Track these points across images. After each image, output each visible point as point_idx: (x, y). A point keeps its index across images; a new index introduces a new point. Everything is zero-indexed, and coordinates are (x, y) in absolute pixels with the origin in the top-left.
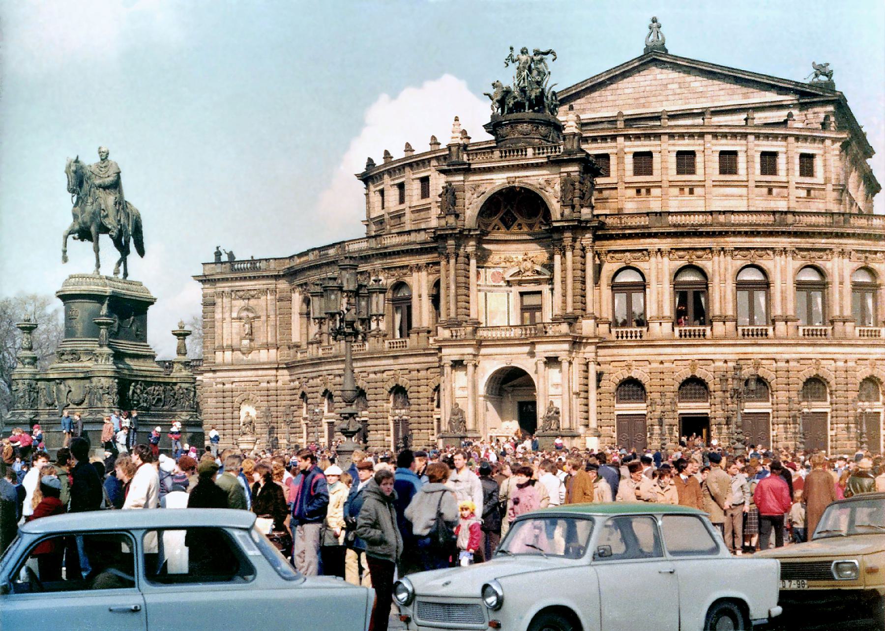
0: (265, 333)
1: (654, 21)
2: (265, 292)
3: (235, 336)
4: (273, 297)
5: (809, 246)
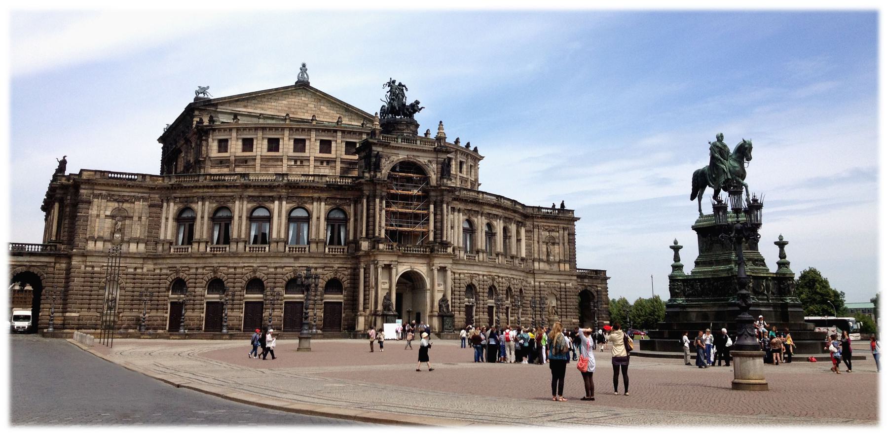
0: (137, 230)
1: (304, 65)
2: (138, 199)
3: (106, 230)
4: (146, 203)
5: (507, 215)
